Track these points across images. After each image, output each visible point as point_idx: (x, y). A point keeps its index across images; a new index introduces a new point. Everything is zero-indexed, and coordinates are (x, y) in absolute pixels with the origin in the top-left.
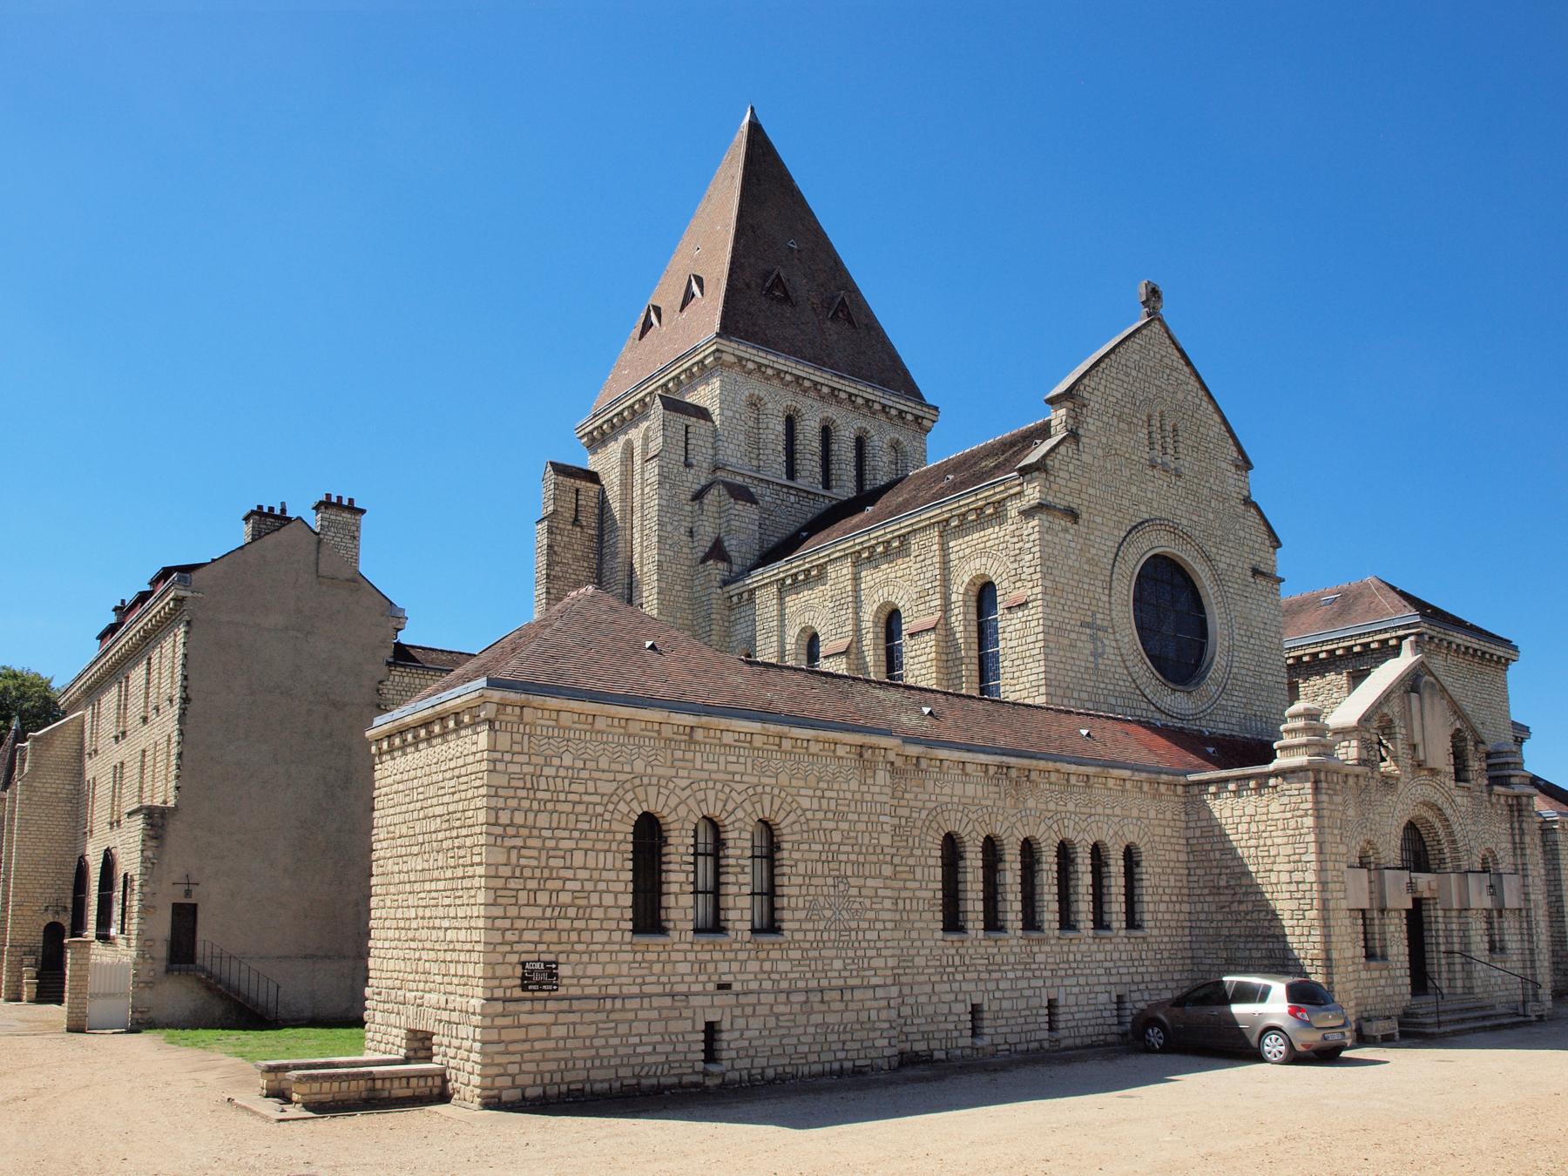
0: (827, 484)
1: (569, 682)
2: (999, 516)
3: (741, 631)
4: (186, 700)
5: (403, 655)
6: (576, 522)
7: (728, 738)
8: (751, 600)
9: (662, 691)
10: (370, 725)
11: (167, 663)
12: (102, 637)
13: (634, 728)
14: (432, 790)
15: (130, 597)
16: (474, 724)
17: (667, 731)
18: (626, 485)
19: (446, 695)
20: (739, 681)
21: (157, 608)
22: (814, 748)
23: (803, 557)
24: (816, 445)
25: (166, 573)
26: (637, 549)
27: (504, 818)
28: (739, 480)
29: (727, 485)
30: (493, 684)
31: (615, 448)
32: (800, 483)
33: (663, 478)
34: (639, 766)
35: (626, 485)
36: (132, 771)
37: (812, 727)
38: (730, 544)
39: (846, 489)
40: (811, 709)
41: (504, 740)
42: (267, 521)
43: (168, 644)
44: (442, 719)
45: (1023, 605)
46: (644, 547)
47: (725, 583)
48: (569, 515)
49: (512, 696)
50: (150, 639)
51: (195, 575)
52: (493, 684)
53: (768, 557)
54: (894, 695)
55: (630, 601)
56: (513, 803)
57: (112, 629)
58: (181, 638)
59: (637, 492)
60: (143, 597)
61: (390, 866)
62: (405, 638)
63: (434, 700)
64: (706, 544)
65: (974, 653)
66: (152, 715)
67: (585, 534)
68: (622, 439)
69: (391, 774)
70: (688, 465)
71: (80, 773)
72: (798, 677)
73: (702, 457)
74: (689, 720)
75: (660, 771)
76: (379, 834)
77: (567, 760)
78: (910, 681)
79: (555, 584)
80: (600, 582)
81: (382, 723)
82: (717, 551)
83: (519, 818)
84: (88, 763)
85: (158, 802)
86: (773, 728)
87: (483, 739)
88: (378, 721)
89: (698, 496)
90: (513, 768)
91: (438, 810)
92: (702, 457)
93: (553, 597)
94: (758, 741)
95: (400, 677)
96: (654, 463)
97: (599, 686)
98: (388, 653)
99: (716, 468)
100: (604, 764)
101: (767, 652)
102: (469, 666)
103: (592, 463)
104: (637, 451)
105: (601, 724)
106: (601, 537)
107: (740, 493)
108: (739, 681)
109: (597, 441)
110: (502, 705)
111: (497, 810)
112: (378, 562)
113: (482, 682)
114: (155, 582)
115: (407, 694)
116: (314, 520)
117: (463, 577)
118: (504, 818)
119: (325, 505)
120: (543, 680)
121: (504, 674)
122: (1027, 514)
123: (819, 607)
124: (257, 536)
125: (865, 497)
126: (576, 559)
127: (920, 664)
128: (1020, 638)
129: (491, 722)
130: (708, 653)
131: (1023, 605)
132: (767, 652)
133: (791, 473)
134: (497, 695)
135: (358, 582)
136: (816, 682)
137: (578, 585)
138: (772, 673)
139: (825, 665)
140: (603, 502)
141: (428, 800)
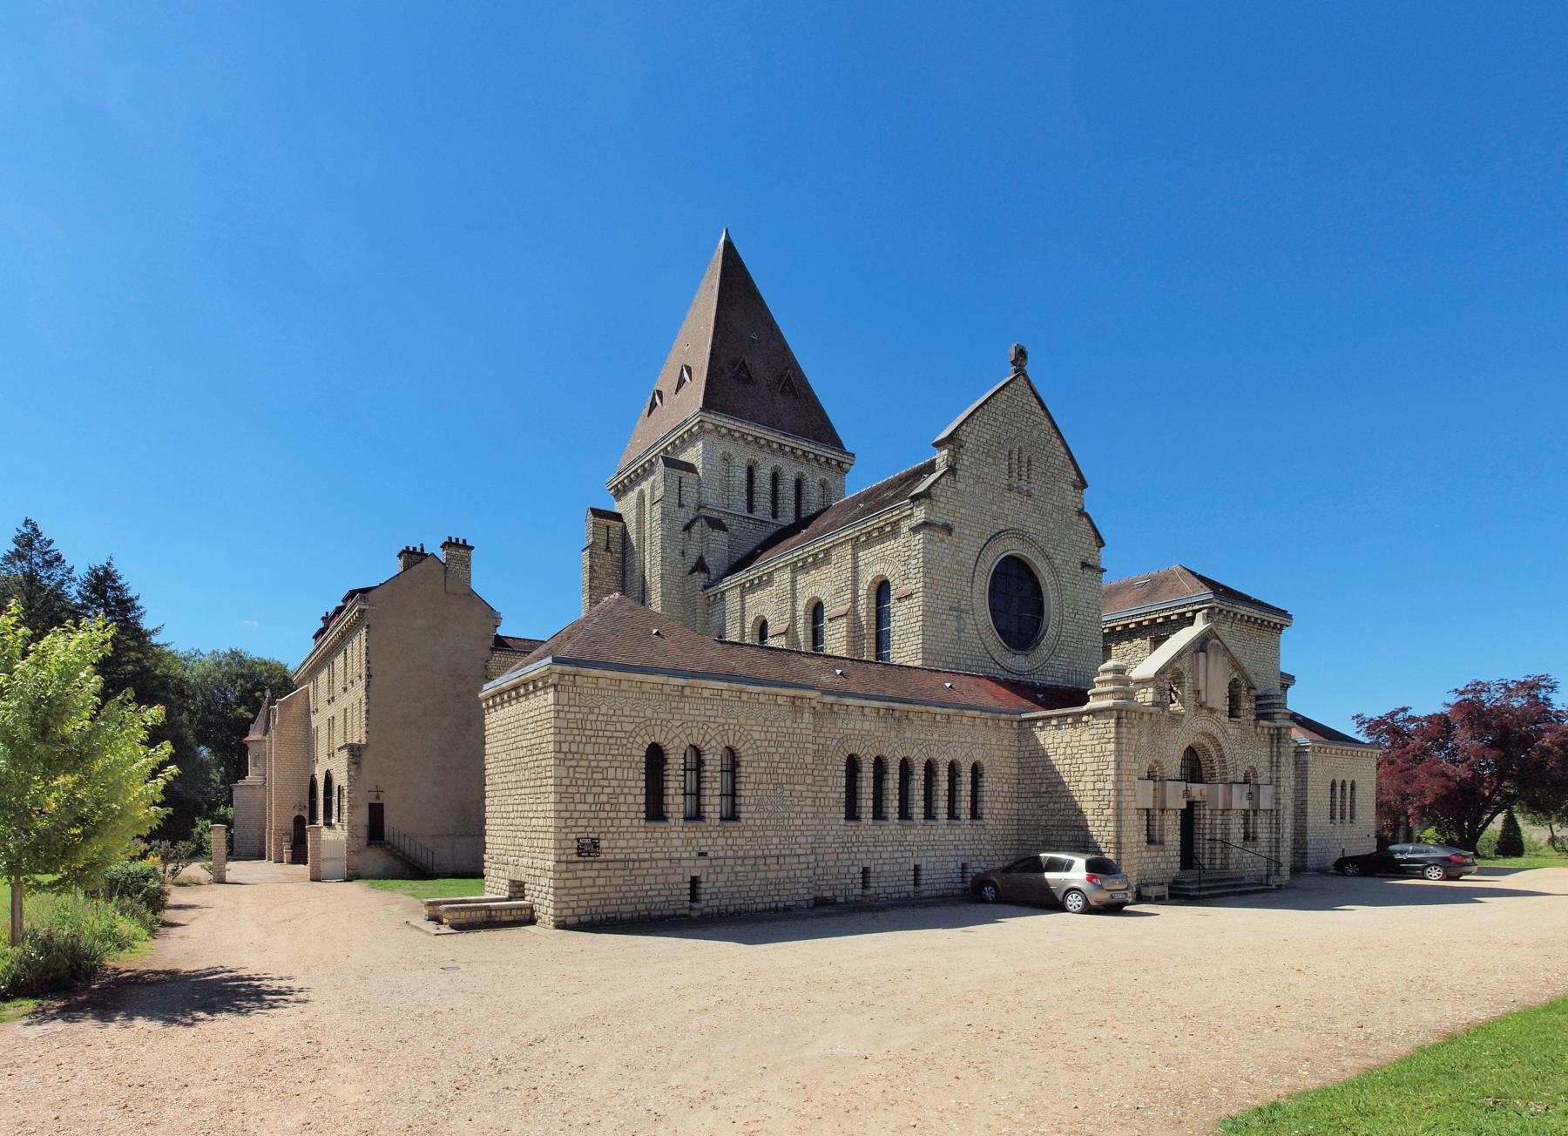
0: (775, 516)
1: (604, 659)
3: (716, 619)
4: (369, 676)
5: (501, 643)
6: (608, 549)
7: (706, 693)
8: (723, 598)
9: (664, 663)
10: (480, 689)
11: (356, 653)
12: (316, 637)
13: (646, 687)
14: (520, 731)
15: (331, 610)
16: (545, 688)
17: (667, 689)
18: (640, 522)
19: (527, 669)
20: (715, 654)
21: (348, 617)
22: (763, 699)
23: (757, 568)
24: (768, 487)
25: (352, 594)
26: (648, 566)
27: (565, 748)
28: (715, 515)
29: (707, 518)
30: (556, 661)
31: (632, 496)
32: (757, 515)
33: (664, 515)
34: (649, 713)
35: (640, 522)
36: (339, 722)
37: (762, 685)
38: (709, 560)
39: (787, 518)
40: (761, 672)
41: (564, 697)
42: (413, 557)
43: (356, 641)
44: (525, 685)
45: (909, 596)
46: (652, 565)
47: (706, 587)
48: (603, 544)
49: (568, 668)
50: (345, 637)
51: (371, 594)
52: (556, 661)
53: (734, 568)
54: (818, 662)
55: (643, 602)
56: (570, 738)
57: (322, 632)
58: (364, 636)
59: (647, 526)
60: (339, 610)
61: (496, 779)
62: (501, 632)
63: (519, 672)
64: (694, 561)
65: (873, 631)
66: (349, 686)
67: (614, 556)
68: (637, 489)
69: (495, 720)
70: (681, 505)
71: (309, 723)
72: (752, 651)
73: (690, 499)
74: (681, 681)
75: (662, 716)
76: (489, 759)
77: (604, 710)
78: (828, 652)
79: (595, 592)
80: (623, 590)
81: (488, 688)
82: (700, 566)
83: (574, 748)
84: (313, 718)
85: (356, 741)
86: (735, 686)
87: (551, 697)
88: (486, 687)
89: (688, 528)
90: (570, 716)
91: (525, 743)
92: (690, 499)
93: (594, 601)
94: (726, 695)
95: (499, 657)
96: (658, 505)
97: (623, 660)
98: (491, 643)
99: (700, 507)
100: (626, 712)
101: (732, 635)
102: (541, 649)
103: (617, 507)
104: (647, 497)
105: (624, 686)
106: (624, 559)
107: (716, 524)
108: (715, 655)
109: (620, 492)
110: (562, 675)
111: (560, 743)
112: (482, 582)
113: (549, 660)
114: (346, 600)
115: (505, 668)
116: (442, 555)
117: (535, 589)
118: (565, 748)
119: (448, 544)
120: (587, 657)
121: (561, 654)
122: (915, 530)
123: (769, 601)
124: (407, 567)
125: (801, 523)
126: (608, 575)
127: (836, 640)
128: (906, 624)
129: (555, 686)
130: (694, 636)
131: (909, 596)
132: (732, 635)
133: (751, 508)
134: (558, 668)
135: (471, 594)
136: (765, 654)
137: (609, 592)
138: (735, 650)
139: (771, 642)
140: (625, 534)
141: (519, 736)
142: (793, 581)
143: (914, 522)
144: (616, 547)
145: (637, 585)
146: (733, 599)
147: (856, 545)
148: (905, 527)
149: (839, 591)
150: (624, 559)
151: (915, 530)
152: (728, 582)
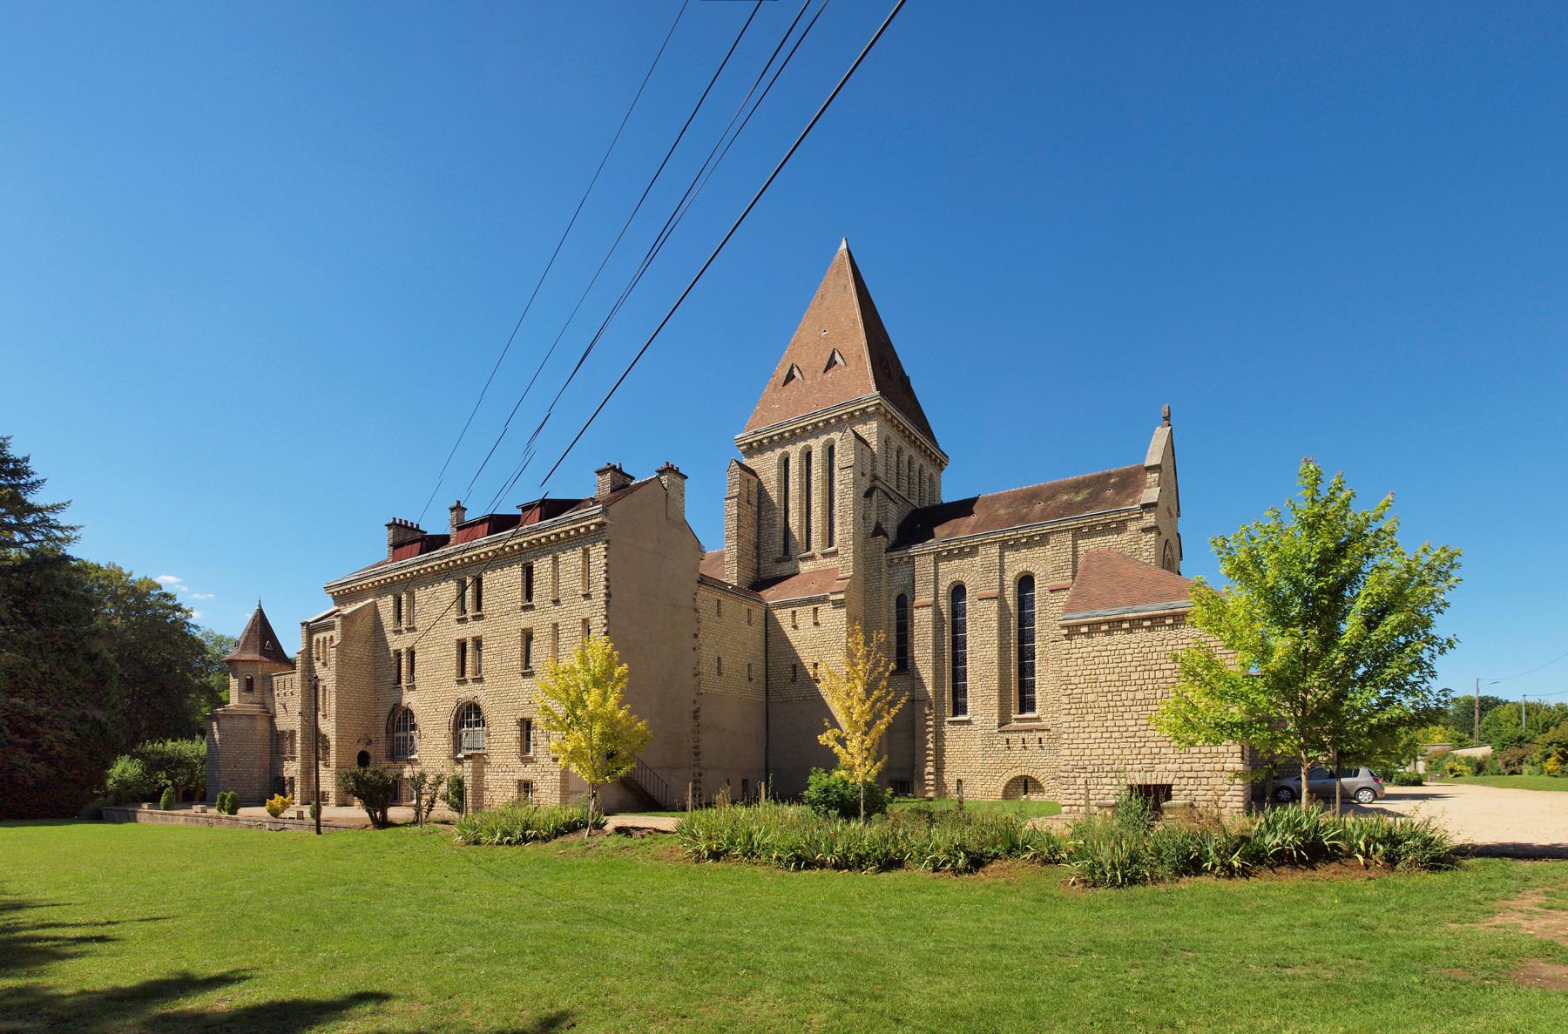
2: (1121, 527)
82: (878, 531)
89: (868, 494)
99: (875, 478)
122: (1145, 530)
142: (1002, 556)
143: (1142, 524)
144: (754, 501)
145: (779, 539)
146: (924, 566)
147: (1078, 533)
148: (1133, 527)
149: (1058, 569)
150: (759, 513)
151: (1145, 530)
152: (916, 549)
